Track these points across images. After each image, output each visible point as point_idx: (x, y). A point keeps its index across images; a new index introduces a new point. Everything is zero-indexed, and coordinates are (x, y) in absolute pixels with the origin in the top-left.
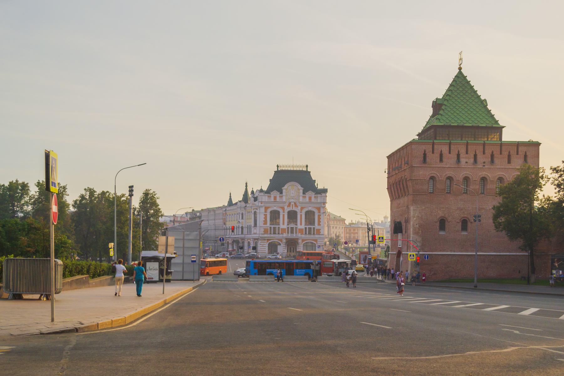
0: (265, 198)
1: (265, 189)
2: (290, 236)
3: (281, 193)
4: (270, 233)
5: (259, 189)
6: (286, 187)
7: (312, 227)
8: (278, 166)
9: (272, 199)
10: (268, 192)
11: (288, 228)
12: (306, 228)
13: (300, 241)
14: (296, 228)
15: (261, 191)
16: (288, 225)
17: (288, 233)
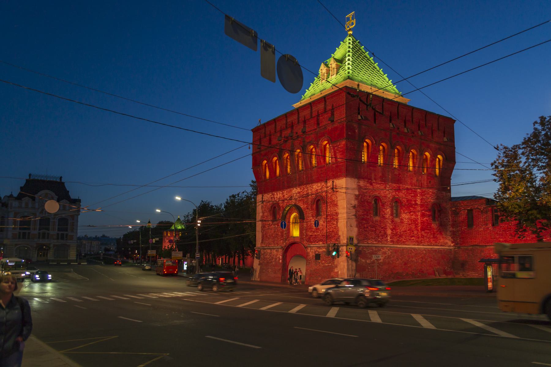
0: (15, 204)
1: (15, 195)
2: (41, 241)
3: (34, 199)
4: (19, 238)
5: (9, 195)
6: (39, 194)
7: (65, 233)
8: (30, 175)
9: (23, 205)
10: (20, 197)
11: (39, 233)
12: (58, 234)
13: (52, 246)
14: (48, 234)
15: (11, 196)
16: (40, 230)
17: (39, 238)
